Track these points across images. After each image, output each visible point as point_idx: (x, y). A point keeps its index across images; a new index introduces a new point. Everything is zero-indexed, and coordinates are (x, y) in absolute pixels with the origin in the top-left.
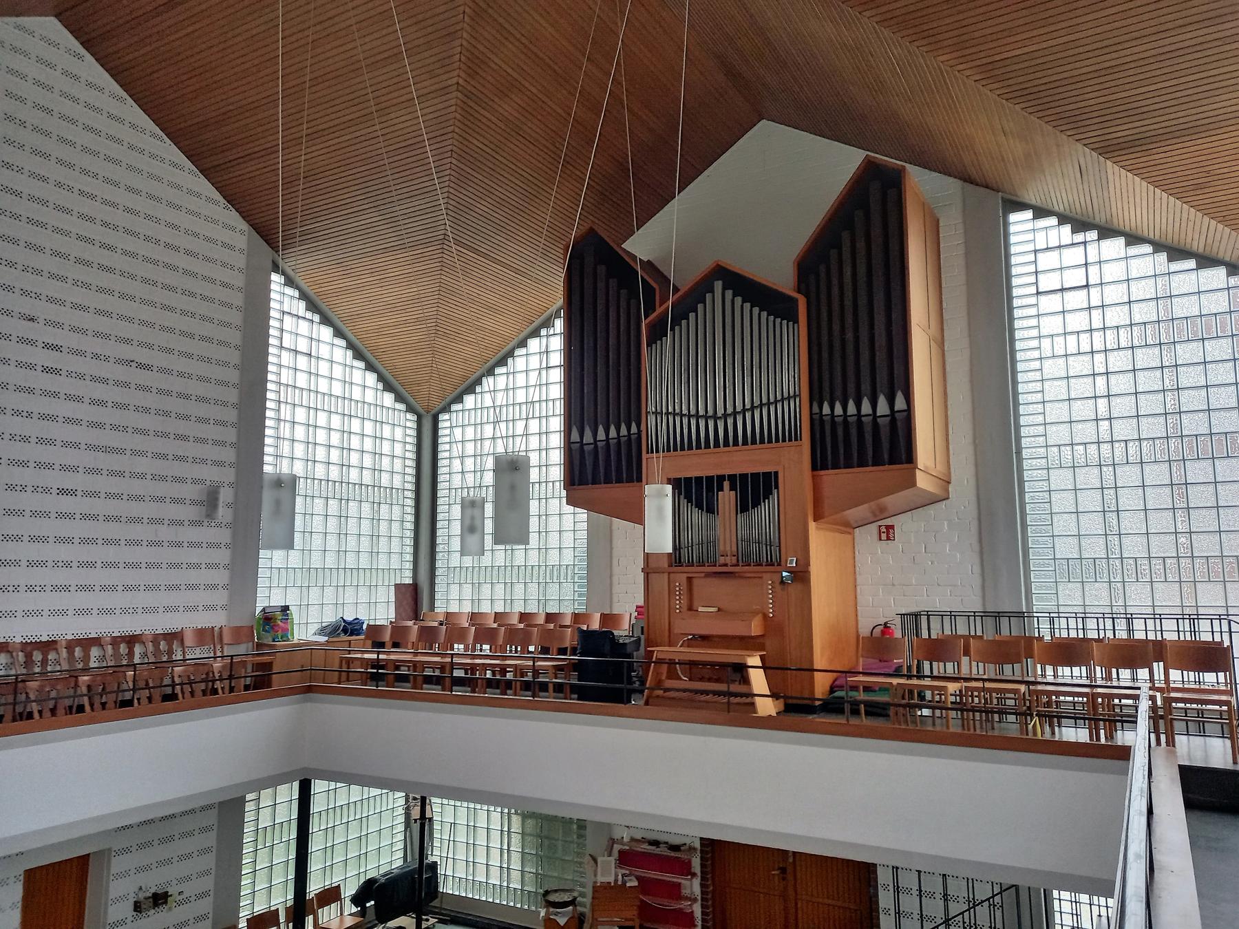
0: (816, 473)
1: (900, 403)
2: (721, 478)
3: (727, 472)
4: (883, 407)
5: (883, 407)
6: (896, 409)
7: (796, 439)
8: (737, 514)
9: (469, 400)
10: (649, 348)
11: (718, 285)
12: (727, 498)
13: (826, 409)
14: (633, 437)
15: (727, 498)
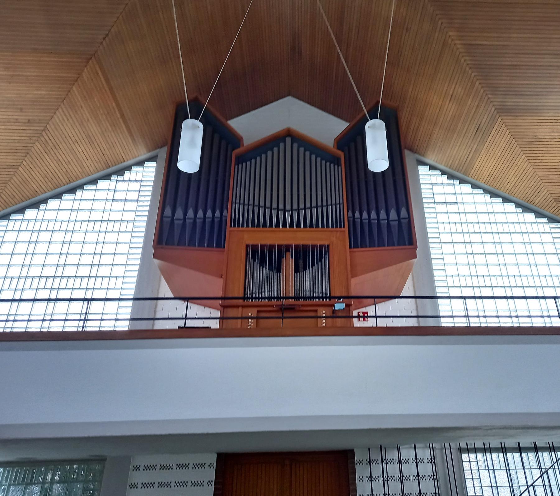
0: (351, 250)
1: (404, 213)
2: (288, 248)
3: (293, 243)
4: (393, 215)
5: (393, 215)
6: (401, 217)
7: (341, 227)
8: (296, 271)
9: (30, 214)
10: (236, 167)
11: (288, 140)
12: (288, 263)
13: (357, 215)
14: (216, 220)
15: (288, 263)
